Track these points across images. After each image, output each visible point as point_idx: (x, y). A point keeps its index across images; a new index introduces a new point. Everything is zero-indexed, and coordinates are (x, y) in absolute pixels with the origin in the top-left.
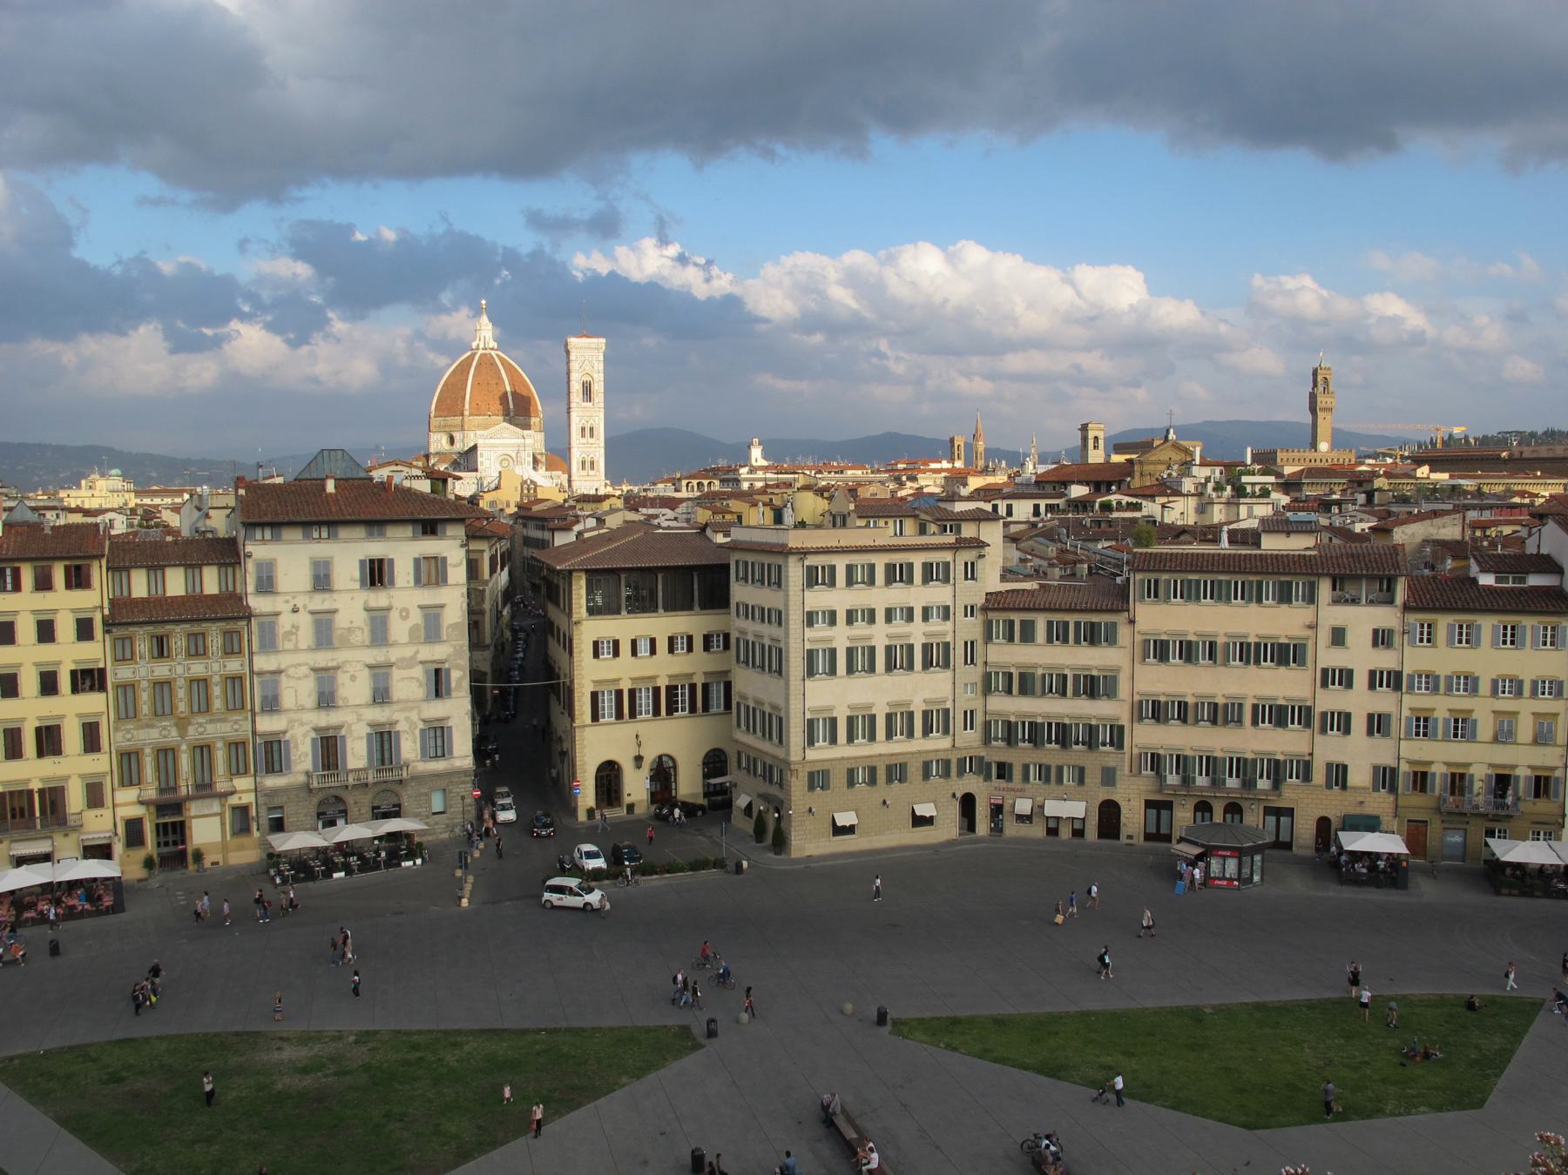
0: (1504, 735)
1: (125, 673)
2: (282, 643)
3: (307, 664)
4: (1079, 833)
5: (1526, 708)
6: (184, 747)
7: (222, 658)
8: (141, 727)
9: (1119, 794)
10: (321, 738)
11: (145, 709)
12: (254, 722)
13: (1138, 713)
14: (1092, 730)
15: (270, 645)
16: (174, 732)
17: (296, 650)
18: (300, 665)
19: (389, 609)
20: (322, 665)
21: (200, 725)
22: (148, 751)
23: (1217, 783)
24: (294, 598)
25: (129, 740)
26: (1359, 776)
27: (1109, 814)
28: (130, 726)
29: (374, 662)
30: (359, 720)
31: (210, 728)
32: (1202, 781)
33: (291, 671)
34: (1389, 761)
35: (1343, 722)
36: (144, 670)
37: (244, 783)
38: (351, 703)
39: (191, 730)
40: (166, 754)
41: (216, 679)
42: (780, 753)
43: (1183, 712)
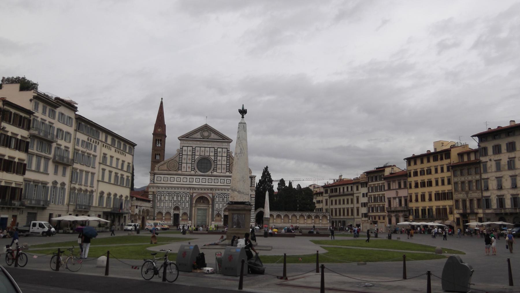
1: (456, 180)
2: (489, 171)
3: (494, 176)
6: (468, 200)
7: (475, 175)
8: (458, 194)
10: (499, 199)
11: (460, 189)
12: (482, 193)
15: (485, 171)
16: (465, 196)
17: (492, 172)
18: (493, 176)
19: (515, 158)
20: (498, 176)
21: (471, 193)
22: (460, 200)
24: (491, 157)
25: (457, 197)
28: (457, 193)
29: (512, 175)
30: (509, 193)
31: (473, 194)
33: (491, 178)
36: (459, 179)
37: (480, 211)
38: (506, 188)
39: (469, 195)
40: (464, 201)
41: (474, 181)
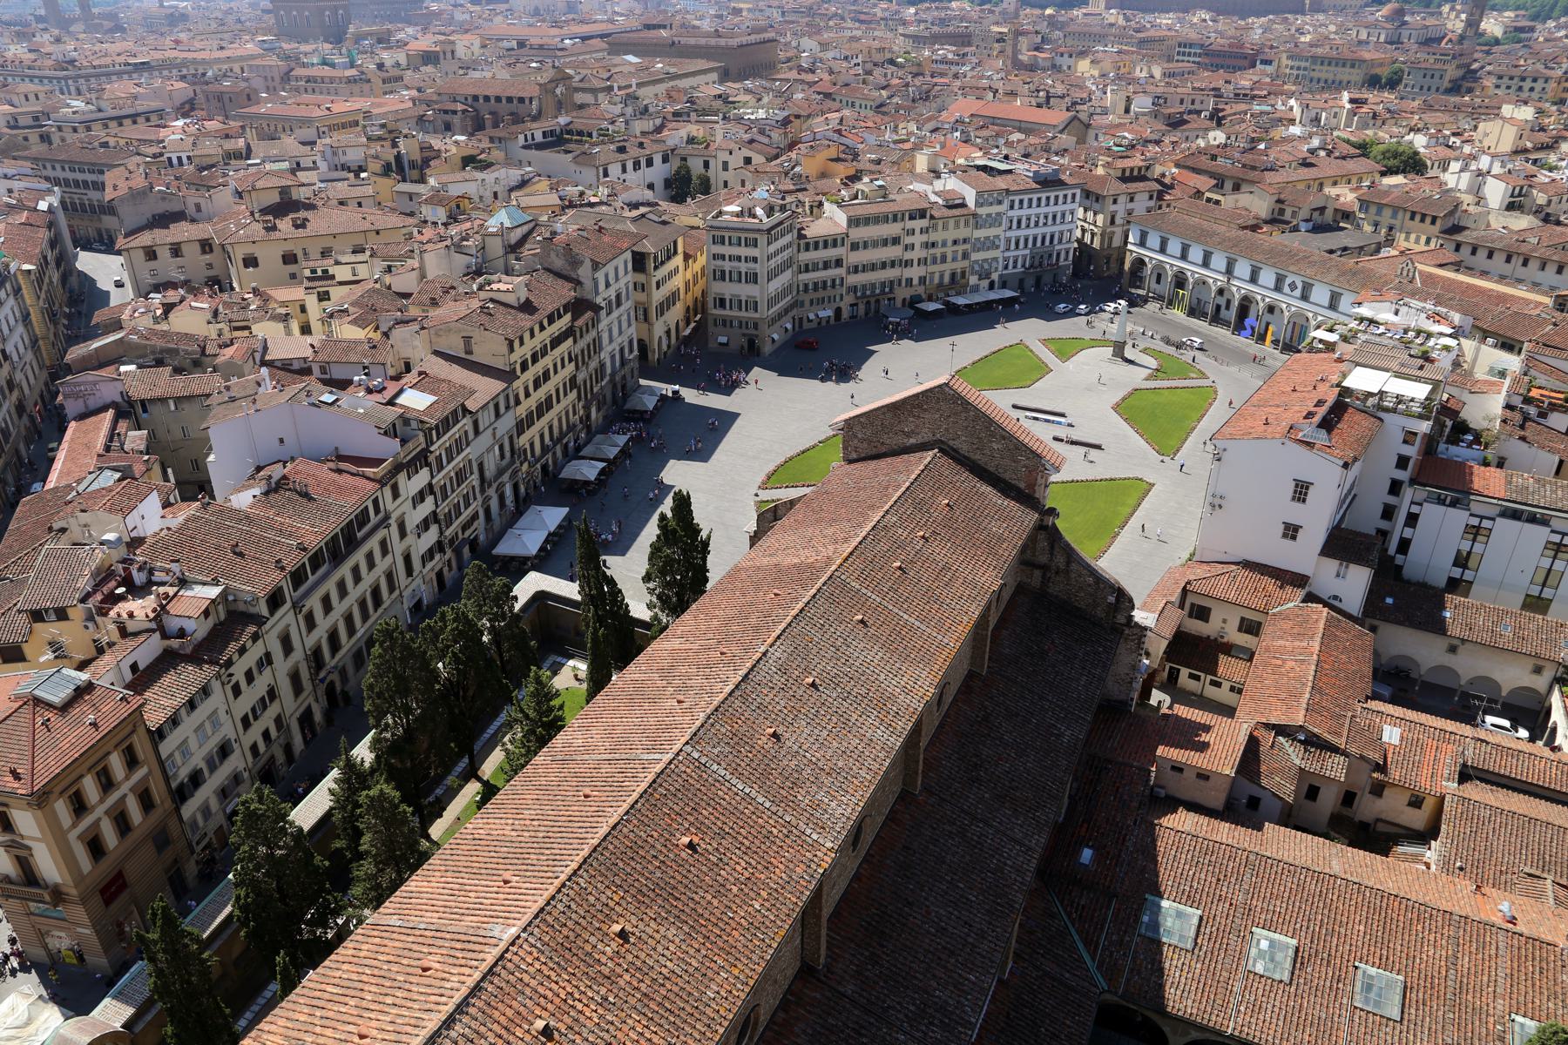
0: (954, 259)
4: (828, 322)
5: (960, 248)
9: (842, 305)
13: (849, 272)
14: (825, 283)
23: (873, 292)
26: (915, 282)
27: (838, 311)
32: (868, 293)
34: (923, 274)
35: (909, 263)
42: (757, 315)
43: (865, 269)
